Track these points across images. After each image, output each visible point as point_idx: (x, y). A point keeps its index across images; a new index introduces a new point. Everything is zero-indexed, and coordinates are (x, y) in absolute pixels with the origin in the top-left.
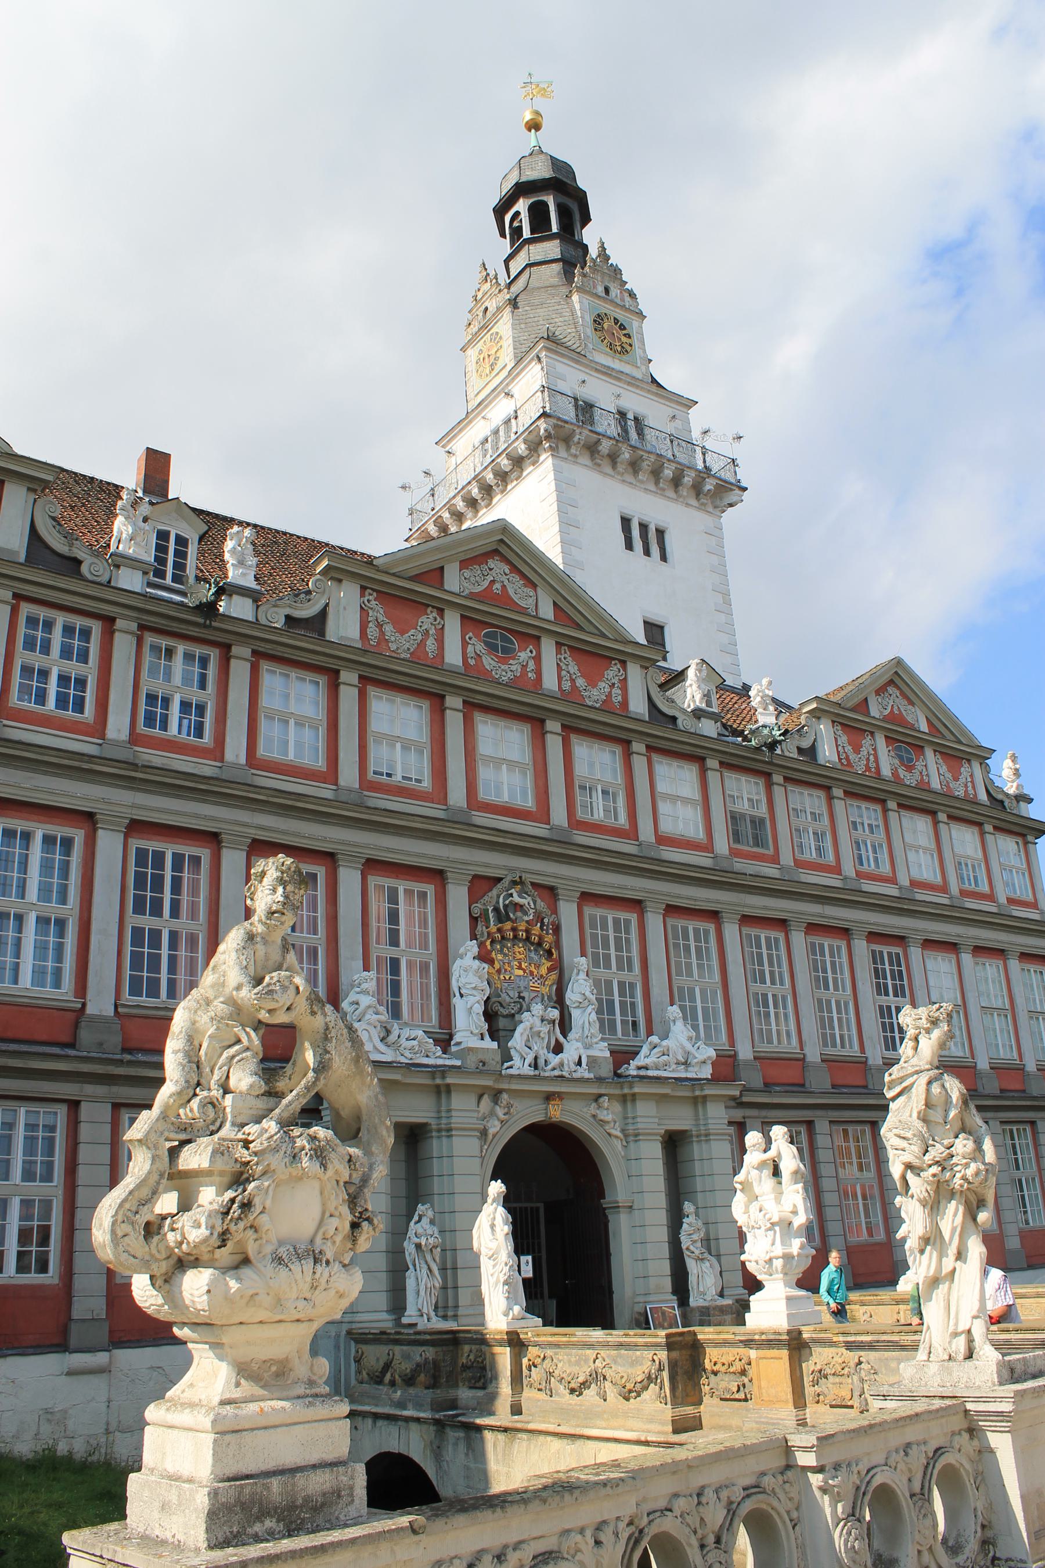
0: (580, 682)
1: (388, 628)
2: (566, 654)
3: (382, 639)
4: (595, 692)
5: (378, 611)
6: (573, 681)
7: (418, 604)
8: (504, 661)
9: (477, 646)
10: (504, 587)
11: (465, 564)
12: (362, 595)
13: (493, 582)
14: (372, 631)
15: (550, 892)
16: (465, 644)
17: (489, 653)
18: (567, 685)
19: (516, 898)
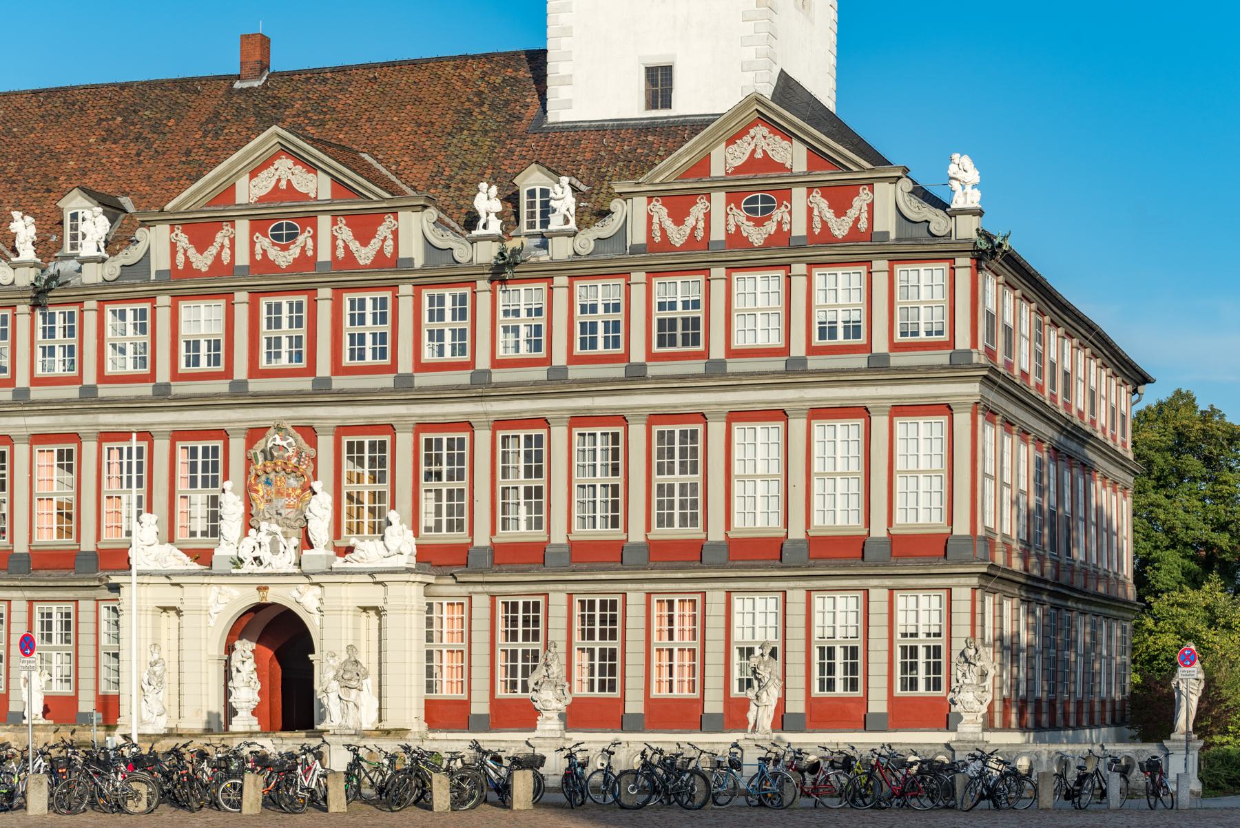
0: (354, 246)
1: (192, 252)
2: (342, 222)
3: (188, 262)
4: (364, 250)
5: (183, 240)
6: (346, 247)
7: (216, 224)
8: (285, 248)
9: (263, 242)
10: (289, 182)
11: (254, 174)
12: (172, 231)
13: (279, 180)
14: (180, 259)
15: (309, 433)
16: (252, 244)
17: (274, 244)
18: (340, 253)
19: (279, 442)
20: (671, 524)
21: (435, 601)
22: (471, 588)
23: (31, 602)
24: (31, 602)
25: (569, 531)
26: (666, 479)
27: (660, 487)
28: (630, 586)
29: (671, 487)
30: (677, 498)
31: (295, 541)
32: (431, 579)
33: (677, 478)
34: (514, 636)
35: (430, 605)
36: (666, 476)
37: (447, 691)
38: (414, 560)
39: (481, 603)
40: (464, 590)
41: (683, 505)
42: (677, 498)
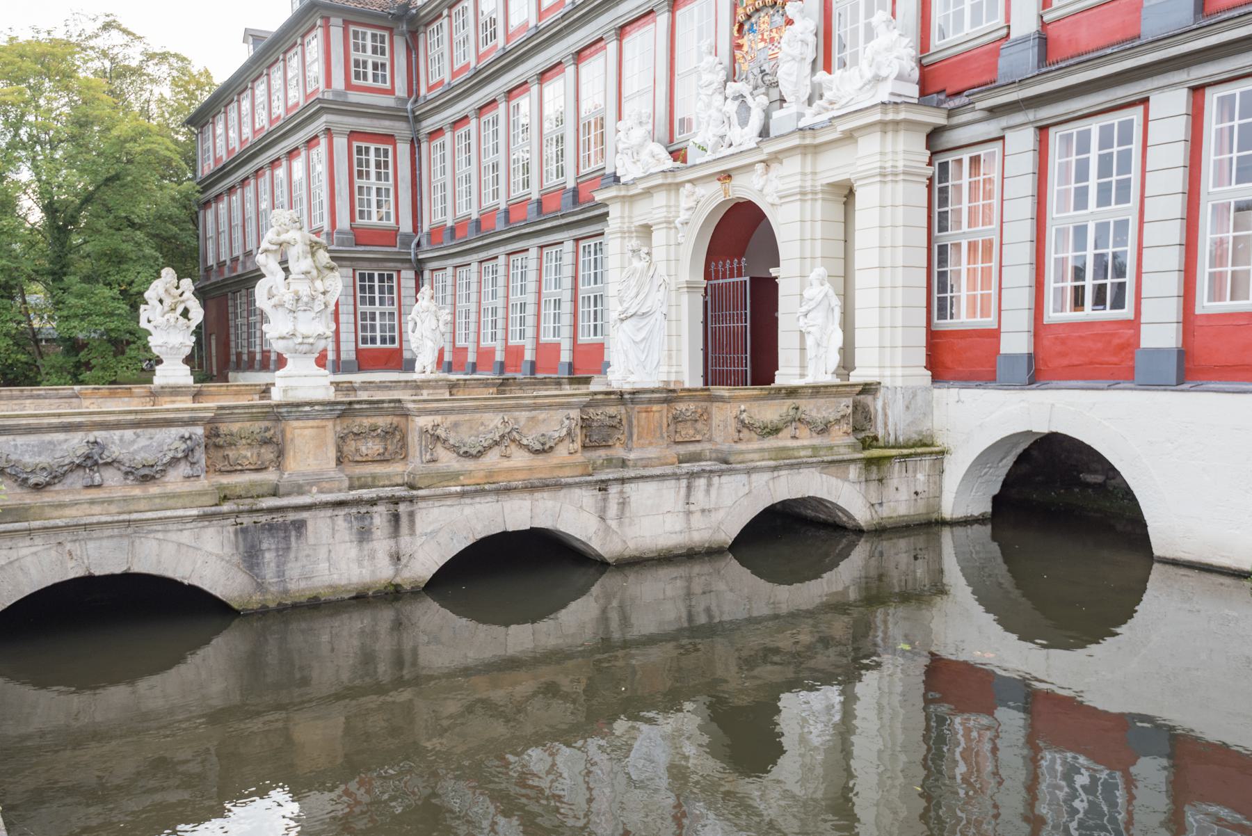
21: (950, 158)
22: (1004, 121)
23: (577, 240)
24: (577, 240)
31: (764, 100)
32: (939, 119)
35: (944, 167)
37: (963, 318)
38: (914, 91)
40: (991, 128)
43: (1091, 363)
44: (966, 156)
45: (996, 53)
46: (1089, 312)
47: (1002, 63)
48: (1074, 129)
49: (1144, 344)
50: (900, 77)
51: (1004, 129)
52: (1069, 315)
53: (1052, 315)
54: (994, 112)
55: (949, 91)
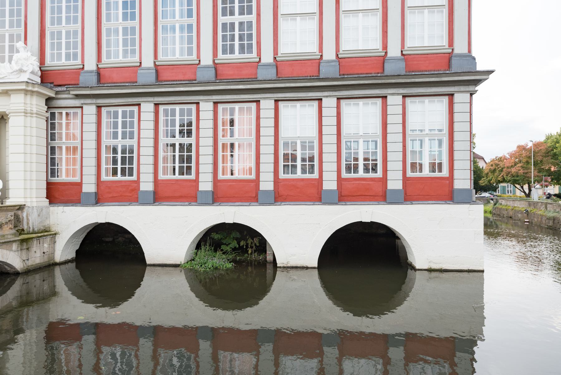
20: (232, 52)
21: (56, 111)
22: (82, 101)
25: (156, 57)
26: (228, 19)
27: (224, 25)
28: (201, 97)
29: (232, 25)
30: (237, 33)
33: (237, 18)
34: (115, 136)
35: (53, 115)
36: (228, 17)
37: (63, 177)
38: (39, 80)
39: (90, 110)
40: (77, 102)
41: (241, 38)
42: (237, 33)
43: (121, 196)
44: (64, 112)
45: (79, 74)
46: (119, 177)
47: (81, 78)
48: (112, 109)
49: (141, 189)
50: (32, 73)
51: (82, 104)
52: (111, 178)
53: (104, 178)
54: (78, 96)
55: (55, 83)
